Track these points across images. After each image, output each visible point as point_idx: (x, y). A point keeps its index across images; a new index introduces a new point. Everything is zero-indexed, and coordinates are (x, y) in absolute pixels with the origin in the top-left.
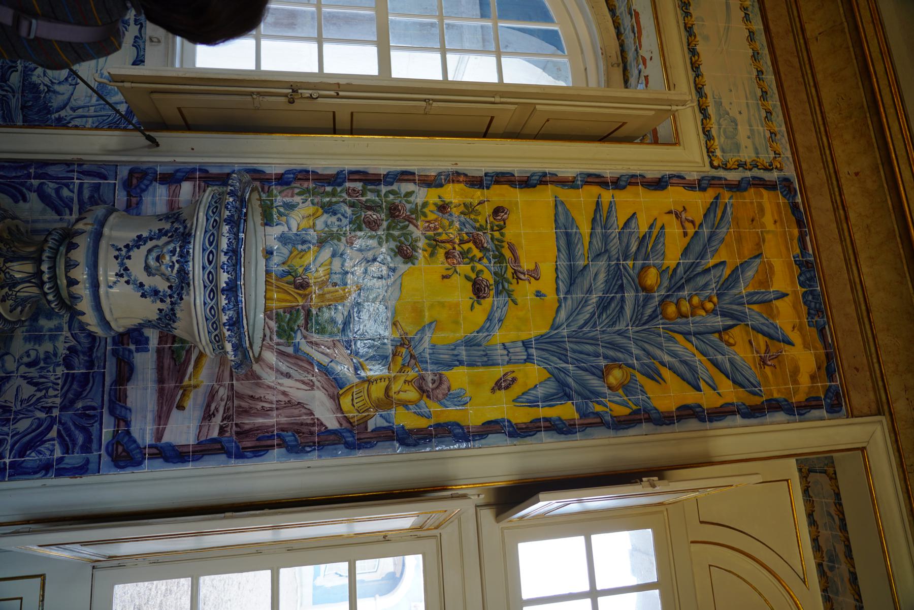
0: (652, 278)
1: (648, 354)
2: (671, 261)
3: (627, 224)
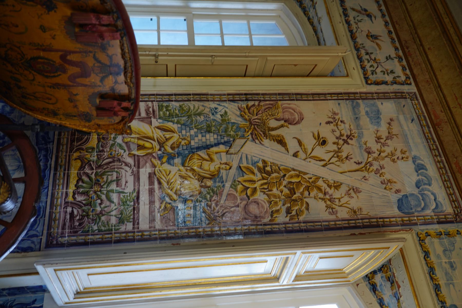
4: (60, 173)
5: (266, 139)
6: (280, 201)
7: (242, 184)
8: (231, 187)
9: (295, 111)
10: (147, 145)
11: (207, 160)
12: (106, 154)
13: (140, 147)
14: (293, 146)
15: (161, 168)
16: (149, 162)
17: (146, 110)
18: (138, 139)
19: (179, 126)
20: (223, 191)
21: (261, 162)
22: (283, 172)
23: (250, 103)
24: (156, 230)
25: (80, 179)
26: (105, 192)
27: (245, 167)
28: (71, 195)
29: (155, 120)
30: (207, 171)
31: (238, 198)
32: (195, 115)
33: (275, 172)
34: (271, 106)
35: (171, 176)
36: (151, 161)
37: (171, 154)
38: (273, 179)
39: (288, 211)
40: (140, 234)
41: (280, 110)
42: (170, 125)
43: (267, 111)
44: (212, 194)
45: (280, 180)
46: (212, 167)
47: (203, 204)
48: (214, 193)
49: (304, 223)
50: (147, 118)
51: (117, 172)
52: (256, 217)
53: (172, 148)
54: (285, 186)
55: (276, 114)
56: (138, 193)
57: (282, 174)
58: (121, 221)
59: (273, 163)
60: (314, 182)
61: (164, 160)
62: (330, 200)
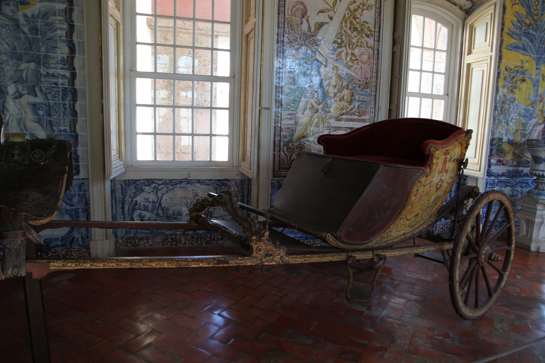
3: (514, 25)
5: (317, 36)
6: (361, 40)
7: (348, 62)
8: (349, 69)
9: (295, 7)
10: (316, 120)
14: (323, 18)
18: (311, 125)
20: (351, 75)
21: (334, 45)
22: (342, 31)
24: (370, 119)
31: (356, 66)
33: (342, 36)
34: (289, 24)
35: (339, 107)
37: (324, 105)
39: (368, 36)
42: (302, 105)
43: (294, 29)
44: (353, 82)
45: (348, 35)
47: (358, 89)
48: (353, 81)
49: (375, 28)
52: (369, 58)
54: (352, 33)
55: (297, 22)
56: (347, 128)
57: (344, 32)
59: (335, 36)
61: (328, 110)
62: (364, 6)
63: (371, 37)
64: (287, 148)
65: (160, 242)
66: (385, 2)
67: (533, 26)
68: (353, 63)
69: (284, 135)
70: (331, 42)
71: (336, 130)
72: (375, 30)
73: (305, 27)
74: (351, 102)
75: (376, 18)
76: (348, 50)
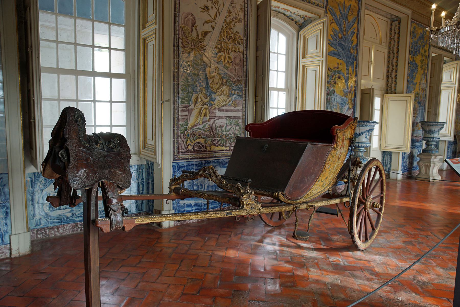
0: (340, 35)
1: (350, 42)
2: (338, 29)
4: (216, 155)
7: (226, 64)
8: (227, 69)
9: (187, 17)
10: (204, 112)
11: (214, 80)
12: (208, 134)
13: (205, 115)
14: (207, 27)
15: (217, 105)
16: (213, 111)
17: (184, 112)
18: (201, 116)
19: (194, 92)
21: (216, 50)
23: (180, 45)
25: (220, 145)
26: (226, 133)
27: (218, 60)
28: (226, 148)
29: (190, 106)
30: (219, 81)
31: (232, 67)
32: (188, 82)
33: (221, 43)
34: (183, 32)
36: (212, 110)
38: (224, 46)
39: (239, 43)
40: (243, 116)
41: (186, 26)
44: (230, 80)
46: (217, 77)
48: (229, 79)
49: (244, 38)
50: (189, 112)
51: (217, 128)
52: (240, 60)
53: (206, 98)
54: (228, 41)
56: (227, 117)
57: (222, 40)
58: (238, 125)
60: (227, 24)
61: (212, 103)
62: (236, 19)
63: (242, 45)
64: (183, 135)
65: (70, 229)
66: (251, 17)
67: (343, 39)
68: (229, 64)
69: (181, 125)
70: (214, 48)
71: (219, 119)
72: (244, 39)
73: (194, 34)
74: (229, 96)
75: (244, 29)
76: (226, 54)
